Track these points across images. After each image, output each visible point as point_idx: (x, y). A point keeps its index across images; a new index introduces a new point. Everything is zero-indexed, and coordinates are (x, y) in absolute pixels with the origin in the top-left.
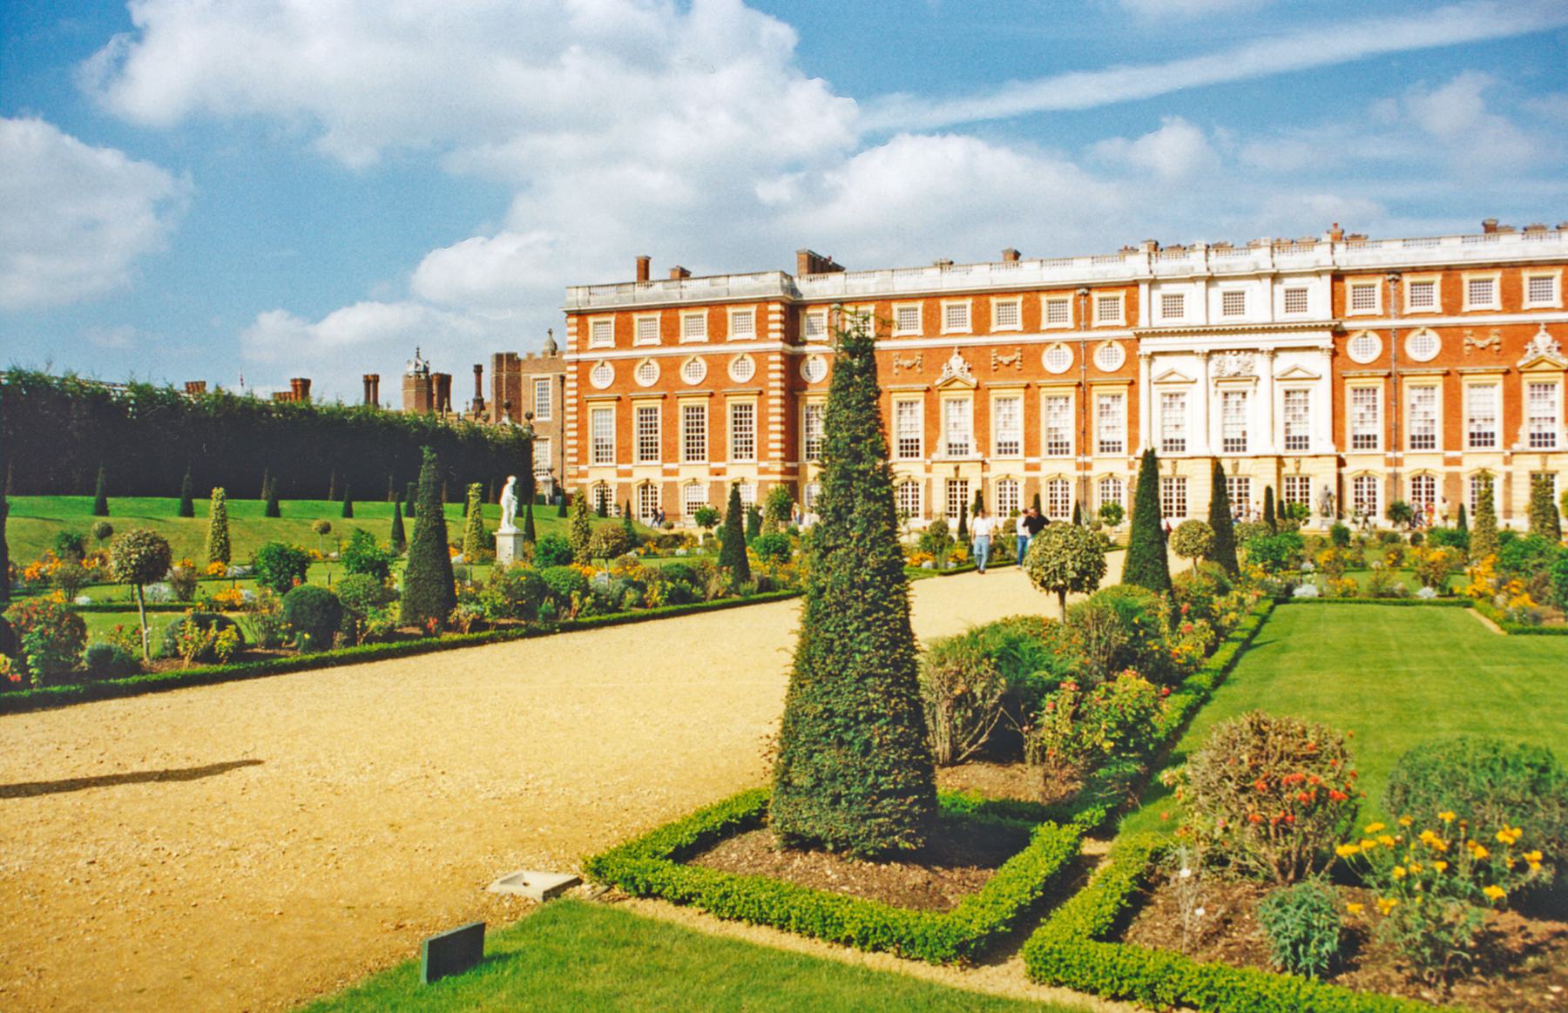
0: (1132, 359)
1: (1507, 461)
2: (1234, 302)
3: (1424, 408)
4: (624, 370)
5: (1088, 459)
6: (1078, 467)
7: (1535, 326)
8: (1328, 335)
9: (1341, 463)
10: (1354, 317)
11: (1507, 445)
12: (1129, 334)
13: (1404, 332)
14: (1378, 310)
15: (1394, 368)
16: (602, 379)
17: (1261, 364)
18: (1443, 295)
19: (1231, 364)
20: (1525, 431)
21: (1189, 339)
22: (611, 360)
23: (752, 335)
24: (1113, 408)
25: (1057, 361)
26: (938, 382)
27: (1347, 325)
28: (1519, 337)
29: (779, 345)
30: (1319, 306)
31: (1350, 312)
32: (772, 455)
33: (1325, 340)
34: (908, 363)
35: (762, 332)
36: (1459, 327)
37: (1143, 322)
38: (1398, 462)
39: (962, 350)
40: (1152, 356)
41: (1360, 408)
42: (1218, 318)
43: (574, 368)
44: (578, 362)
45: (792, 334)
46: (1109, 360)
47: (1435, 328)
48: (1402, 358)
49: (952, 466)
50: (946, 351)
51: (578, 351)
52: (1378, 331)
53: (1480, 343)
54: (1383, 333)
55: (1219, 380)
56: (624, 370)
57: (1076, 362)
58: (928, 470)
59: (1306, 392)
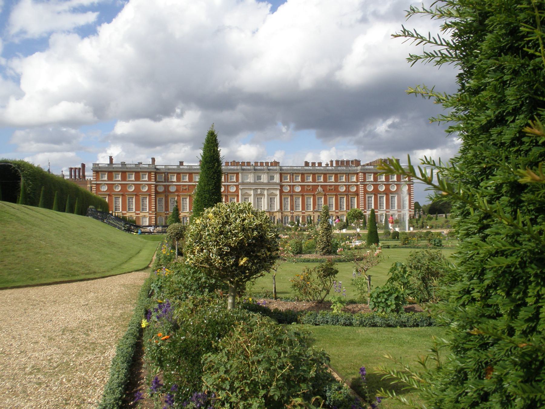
0: (237, 191)
1: (314, 213)
2: (259, 178)
7: (318, 185)
9: (282, 213)
12: (237, 184)
13: (294, 186)
14: (288, 180)
15: (292, 193)
20: (316, 207)
22: (107, 184)
29: (154, 183)
30: (277, 179)
31: (283, 181)
35: (150, 179)
36: (304, 185)
37: (240, 181)
40: (241, 189)
47: (300, 185)
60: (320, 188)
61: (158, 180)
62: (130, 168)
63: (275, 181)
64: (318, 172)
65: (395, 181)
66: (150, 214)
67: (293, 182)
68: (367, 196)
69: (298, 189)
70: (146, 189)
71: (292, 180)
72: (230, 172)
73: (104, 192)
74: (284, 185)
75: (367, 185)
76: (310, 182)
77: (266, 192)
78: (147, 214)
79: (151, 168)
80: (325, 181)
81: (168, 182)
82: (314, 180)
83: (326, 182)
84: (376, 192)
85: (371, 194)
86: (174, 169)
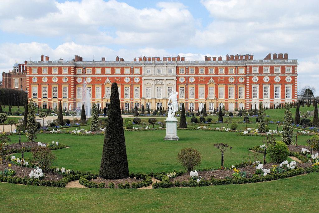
2: (159, 70)
3: (192, 89)
4: (40, 79)
5: (133, 99)
6: (131, 100)
7: (210, 77)
8: (176, 77)
10: (180, 74)
11: (206, 98)
12: (140, 76)
13: (189, 77)
14: (184, 73)
16: (35, 80)
17: (164, 83)
18: (195, 71)
19: (159, 82)
21: (151, 77)
22: (37, 77)
23: (67, 73)
24: (138, 89)
25: (127, 80)
26: (104, 84)
27: (179, 76)
28: (208, 79)
29: (73, 75)
30: (174, 72)
31: (180, 73)
32: (71, 97)
33: (175, 78)
34: (99, 80)
35: (70, 73)
36: (198, 77)
37: (143, 73)
38: (188, 100)
39: (109, 77)
41: (181, 91)
42: (156, 73)
43: (28, 78)
44: (29, 77)
45: (75, 73)
46: (137, 80)
47: (194, 77)
48: (188, 82)
49: (107, 100)
50: (106, 78)
51: (29, 74)
52: (184, 77)
53: (201, 80)
54: (185, 77)
55: (156, 85)
56: (40, 79)
57: (131, 80)
58: (102, 100)
59: (172, 88)
60: (211, 80)
61: (77, 73)
62: (55, 64)
63: (173, 73)
64: (210, 65)
65: (279, 74)
66: (69, 100)
67: (188, 74)
68: (253, 86)
69: (192, 80)
70: (65, 80)
71: (187, 72)
72: (135, 66)
73: (35, 83)
74: (179, 77)
75: (252, 77)
76: (204, 74)
77: (164, 83)
78: (67, 101)
79: (71, 64)
80: (217, 72)
81: (85, 75)
82: (207, 72)
83: (217, 75)
84: (261, 82)
85: (257, 84)
86: (90, 64)
